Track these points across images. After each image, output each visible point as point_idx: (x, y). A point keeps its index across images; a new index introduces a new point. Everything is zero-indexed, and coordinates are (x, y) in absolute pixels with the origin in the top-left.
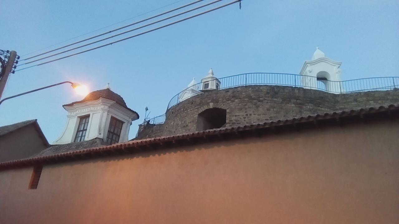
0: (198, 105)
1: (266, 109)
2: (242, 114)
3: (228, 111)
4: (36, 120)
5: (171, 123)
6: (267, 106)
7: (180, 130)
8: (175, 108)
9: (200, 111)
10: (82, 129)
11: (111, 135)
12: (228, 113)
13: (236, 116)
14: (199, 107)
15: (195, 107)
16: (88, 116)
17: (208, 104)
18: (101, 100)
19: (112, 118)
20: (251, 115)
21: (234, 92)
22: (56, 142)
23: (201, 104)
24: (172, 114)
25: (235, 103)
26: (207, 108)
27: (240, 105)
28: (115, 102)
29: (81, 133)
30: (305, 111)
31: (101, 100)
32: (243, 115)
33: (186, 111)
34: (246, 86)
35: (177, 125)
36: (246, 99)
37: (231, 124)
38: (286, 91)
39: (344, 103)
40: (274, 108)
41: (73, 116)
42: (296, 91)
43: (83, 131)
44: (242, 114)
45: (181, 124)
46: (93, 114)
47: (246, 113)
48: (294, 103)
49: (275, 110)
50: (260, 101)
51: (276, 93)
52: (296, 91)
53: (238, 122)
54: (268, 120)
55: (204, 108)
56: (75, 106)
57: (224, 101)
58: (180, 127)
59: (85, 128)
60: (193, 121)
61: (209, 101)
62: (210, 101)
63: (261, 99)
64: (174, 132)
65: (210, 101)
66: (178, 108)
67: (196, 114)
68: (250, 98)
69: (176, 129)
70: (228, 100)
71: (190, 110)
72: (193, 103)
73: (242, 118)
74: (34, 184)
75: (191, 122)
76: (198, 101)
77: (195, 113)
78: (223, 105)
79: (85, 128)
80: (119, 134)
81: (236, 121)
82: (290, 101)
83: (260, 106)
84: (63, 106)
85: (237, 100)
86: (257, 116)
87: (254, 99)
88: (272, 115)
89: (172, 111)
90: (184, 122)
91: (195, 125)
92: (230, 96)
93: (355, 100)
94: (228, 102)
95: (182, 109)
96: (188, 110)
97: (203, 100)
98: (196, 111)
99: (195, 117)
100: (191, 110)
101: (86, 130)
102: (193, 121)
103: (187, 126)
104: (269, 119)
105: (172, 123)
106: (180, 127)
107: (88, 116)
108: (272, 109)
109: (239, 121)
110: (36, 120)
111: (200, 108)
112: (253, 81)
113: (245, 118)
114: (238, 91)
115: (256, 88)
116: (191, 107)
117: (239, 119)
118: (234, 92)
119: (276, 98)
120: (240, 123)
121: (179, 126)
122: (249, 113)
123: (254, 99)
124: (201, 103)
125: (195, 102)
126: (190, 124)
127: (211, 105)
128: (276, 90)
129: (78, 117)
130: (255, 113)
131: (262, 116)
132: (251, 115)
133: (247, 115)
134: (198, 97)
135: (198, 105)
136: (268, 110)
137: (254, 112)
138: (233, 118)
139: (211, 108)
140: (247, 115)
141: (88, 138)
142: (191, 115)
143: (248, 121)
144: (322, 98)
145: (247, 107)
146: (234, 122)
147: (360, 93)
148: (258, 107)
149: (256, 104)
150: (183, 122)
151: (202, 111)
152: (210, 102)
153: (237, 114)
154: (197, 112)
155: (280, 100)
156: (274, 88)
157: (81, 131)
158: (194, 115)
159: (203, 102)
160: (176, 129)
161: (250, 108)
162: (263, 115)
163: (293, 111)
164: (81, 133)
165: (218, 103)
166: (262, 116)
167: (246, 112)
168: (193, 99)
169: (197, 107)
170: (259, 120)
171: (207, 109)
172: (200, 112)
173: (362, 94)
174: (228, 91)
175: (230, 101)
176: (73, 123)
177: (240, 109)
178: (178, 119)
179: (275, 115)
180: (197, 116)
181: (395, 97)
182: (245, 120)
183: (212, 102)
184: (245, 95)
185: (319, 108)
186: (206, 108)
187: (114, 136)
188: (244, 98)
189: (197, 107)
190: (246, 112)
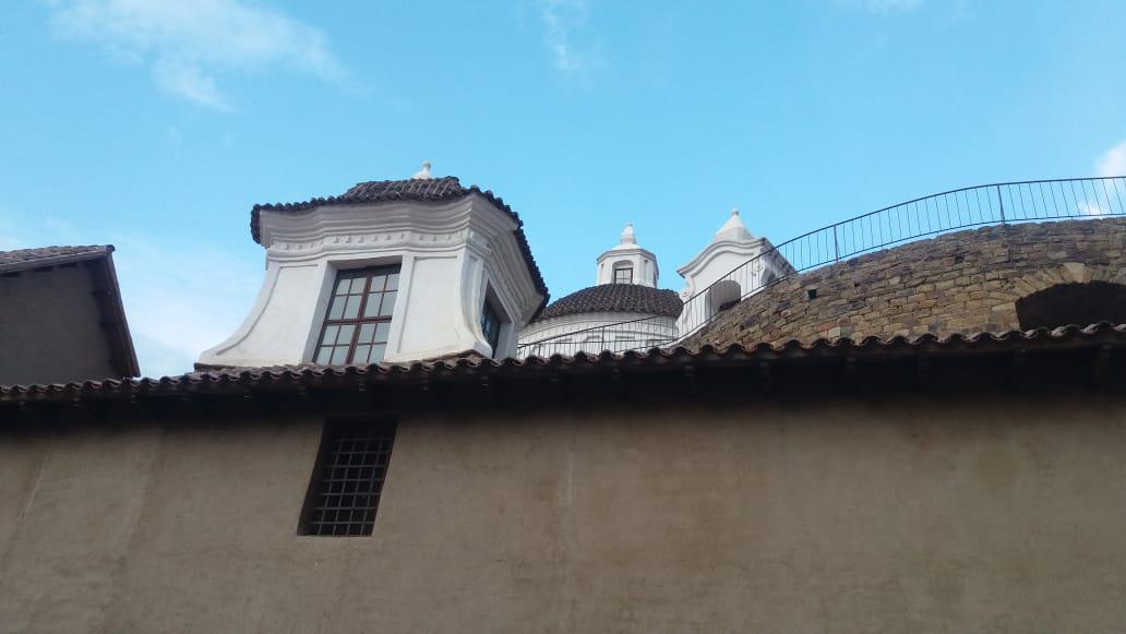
4: (111, 248)
9: (1028, 286)
10: (352, 314)
14: (1013, 275)
15: (984, 271)
16: (393, 267)
17: (1057, 265)
18: (469, 204)
22: (218, 354)
26: (1060, 281)
31: (469, 204)
33: (926, 288)
41: (308, 260)
43: (360, 321)
46: (416, 258)
55: (1040, 279)
56: (321, 216)
59: (370, 312)
62: (1063, 254)
66: (857, 276)
67: (1004, 302)
71: (955, 286)
72: (968, 258)
74: (340, 504)
77: (994, 294)
79: (370, 312)
84: (257, 208)
89: (812, 287)
95: (896, 280)
97: (1023, 249)
98: (996, 290)
99: (994, 309)
100: (964, 280)
101: (389, 319)
107: (393, 267)
110: (111, 248)
111: (1016, 279)
116: (956, 274)
124: (1017, 261)
127: (1077, 273)
129: (330, 263)
135: (998, 267)
139: (1080, 280)
141: (398, 352)
142: (976, 304)
151: (1033, 291)
152: (1068, 260)
154: (1009, 291)
158: (988, 302)
159: (1025, 256)
164: (348, 331)
165: (1110, 268)
168: (962, 244)
169: (1001, 274)
171: (1057, 286)
172: (1025, 295)
176: (304, 288)
178: (875, 315)
180: (1012, 306)
183: (1076, 256)
186: (1045, 280)
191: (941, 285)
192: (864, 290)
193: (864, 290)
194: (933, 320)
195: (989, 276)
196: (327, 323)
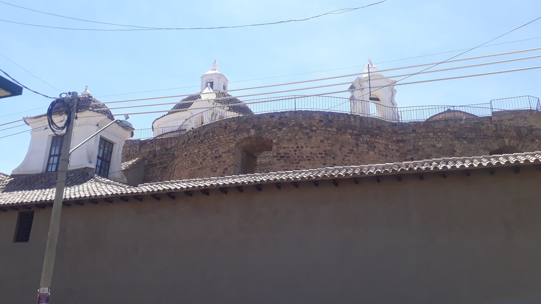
0: (234, 131)
1: (319, 141)
2: (291, 145)
3: (274, 141)
5: (193, 150)
6: (321, 138)
7: (210, 161)
8: (199, 131)
10: (57, 153)
11: (100, 161)
12: (275, 143)
13: (284, 148)
15: (230, 133)
17: (248, 131)
19: (102, 139)
20: (302, 147)
21: (280, 118)
23: (238, 131)
24: (195, 140)
25: (283, 132)
27: (290, 134)
28: (106, 117)
29: (56, 159)
30: (362, 143)
32: (293, 148)
34: (296, 112)
35: (205, 154)
36: (296, 128)
37: (279, 158)
38: (342, 119)
39: (402, 134)
40: (328, 139)
42: (352, 120)
44: (292, 145)
45: (212, 153)
47: (297, 145)
48: (350, 134)
49: (329, 142)
50: (312, 131)
51: (331, 122)
52: (352, 120)
53: (288, 156)
54: (322, 154)
57: (269, 128)
58: (209, 158)
60: (229, 152)
61: (248, 127)
63: (314, 128)
64: (201, 163)
65: (250, 127)
66: (203, 133)
68: (301, 126)
69: (204, 160)
70: (274, 127)
72: (228, 128)
73: (292, 150)
75: (225, 153)
76: (234, 125)
78: (267, 133)
80: (108, 160)
81: (285, 154)
82: (346, 132)
83: (313, 137)
85: (284, 129)
86: (309, 149)
87: (306, 128)
88: (328, 148)
89: (194, 134)
90: (216, 151)
91: (231, 157)
92: (276, 122)
93: (414, 131)
94: (273, 130)
95: (211, 134)
96: (220, 137)
102: (229, 152)
103: (220, 156)
104: (323, 153)
105: (196, 151)
106: (209, 158)
108: (326, 141)
109: (288, 154)
112: (303, 105)
113: (295, 151)
114: (286, 118)
115: (308, 115)
117: (288, 152)
118: (281, 118)
119: (330, 127)
120: (290, 157)
121: (207, 157)
122: (300, 144)
123: (306, 128)
125: (230, 126)
126: (224, 155)
128: (330, 117)
130: (307, 145)
131: (315, 149)
132: (302, 147)
133: (298, 147)
134: (234, 121)
135: (234, 131)
136: (322, 141)
137: (306, 144)
138: (282, 151)
140: (298, 147)
143: (299, 155)
144: (379, 127)
145: (297, 137)
146: (283, 155)
147: (419, 123)
148: (310, 138)
149: (308, 134)
150: (214, 151)
152: (251, 128)
153: (286, 146)
155: (334, 130)
156: (327, 115)
157: (54, 156)
160: (204, 160)
161: (301, 138)
162: (317, 147)
163: (349, 144)
164: (56, 159)
166: (315, 149)
167: (296, 144)
170: (311, 153)
173: (421, 124)
174: (274, 116)
175: (276, 130)
177: (290, 140)
178: (205, 146)
179: (330, 148)
181: (455, 130)
182: (295, 154)
184: (294, 123)
185: (377, 140)
186: (245, 135)
187: (104, 162)
188: (293, 125)
189: (233, 134)
190: (296, 144)
191: (220, 137)
192: (205, 137)
193: (205, 137)
194: (216, 149)
195: (231, 134)
196: (50, 156)
